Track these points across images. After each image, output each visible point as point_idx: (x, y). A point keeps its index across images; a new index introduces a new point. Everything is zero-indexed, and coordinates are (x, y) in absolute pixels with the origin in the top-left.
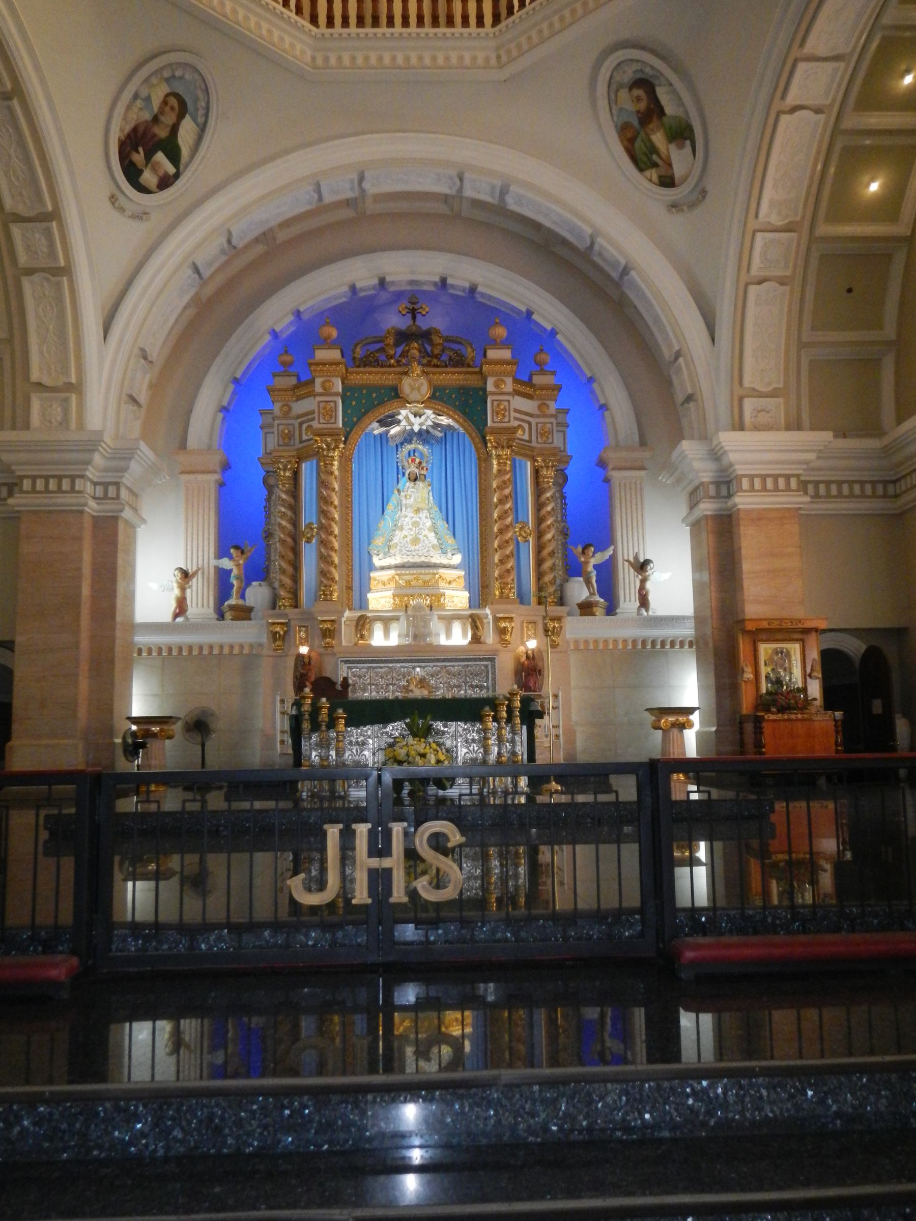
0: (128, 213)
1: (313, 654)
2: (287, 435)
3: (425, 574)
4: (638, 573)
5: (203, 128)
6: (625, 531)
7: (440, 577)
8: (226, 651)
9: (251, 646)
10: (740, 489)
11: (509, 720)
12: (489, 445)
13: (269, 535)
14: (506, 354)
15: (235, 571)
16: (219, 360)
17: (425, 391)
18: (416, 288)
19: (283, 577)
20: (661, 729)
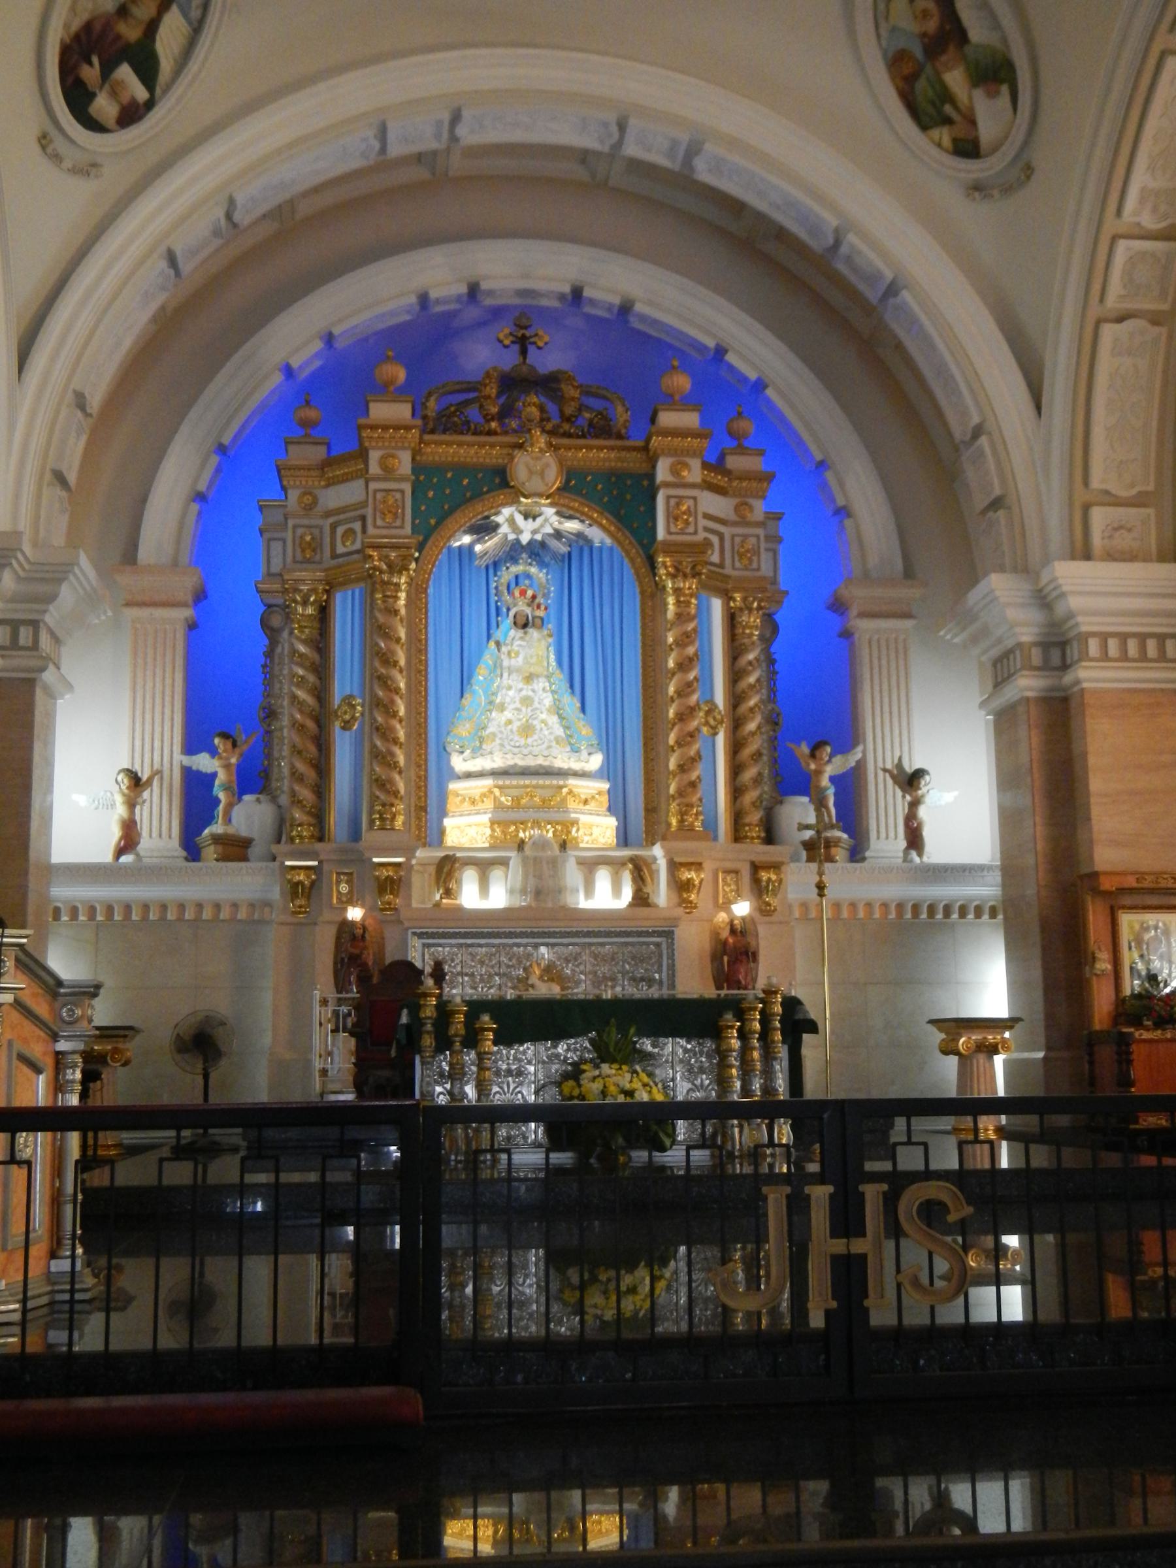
0: (68, 164)
1: (369, 922)
2: (309, 544)
3: (543, 787)
4: (904, 791)
5: (197, 29)
6: (878, 720)
7: (570, 792)
8: (207, 914)
9: (252, 905)
10: (1084, 656)
11: (765, 1035)
12: (662, 571)
13: (270, 714)
14: (690, 419)
15: (222, 776)
16: (193, 414)
17: (553, 478)
18: (529, 301)
19: (297, 788)
20: (957, 1053)
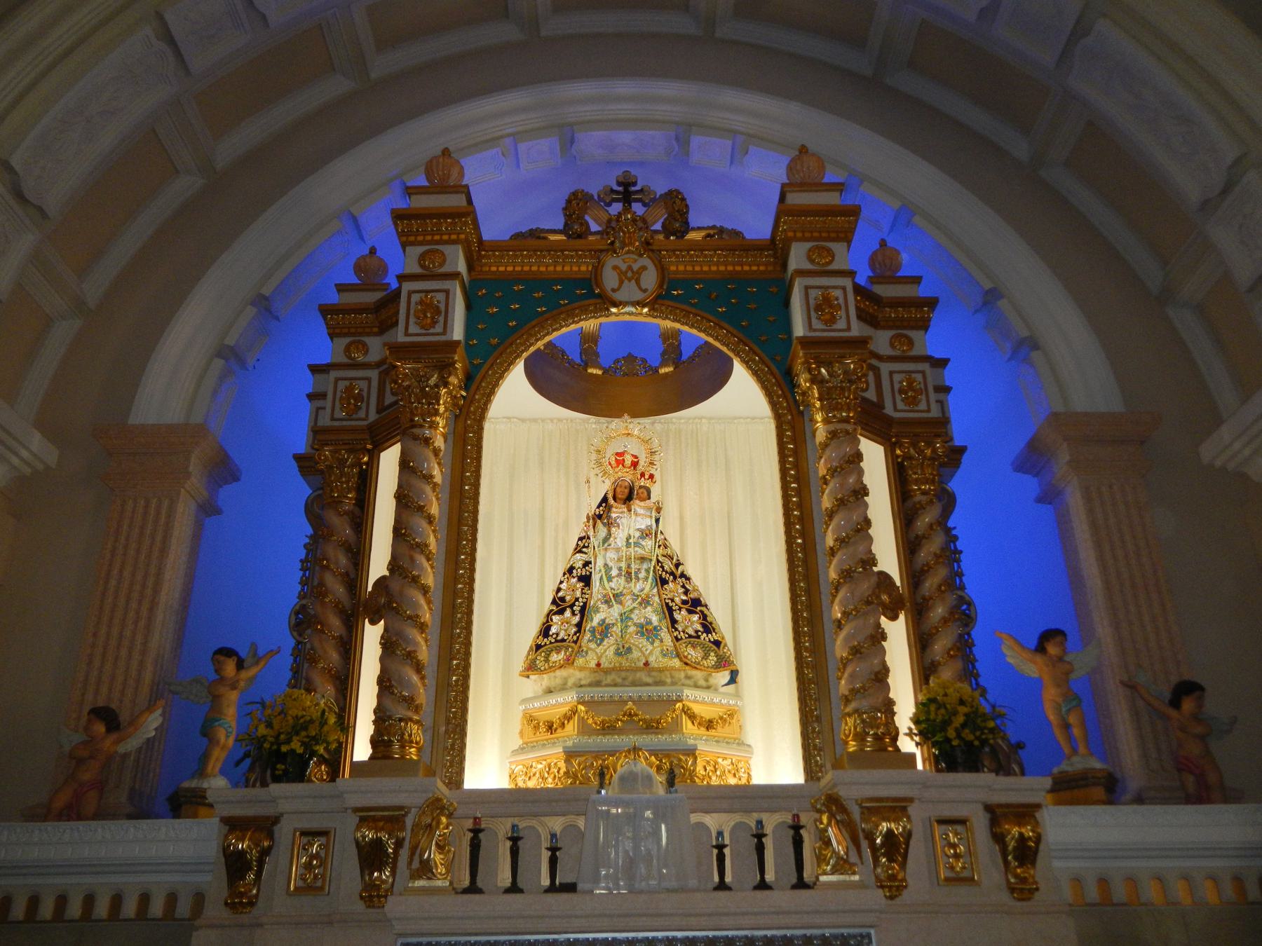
17: (650, 279)
